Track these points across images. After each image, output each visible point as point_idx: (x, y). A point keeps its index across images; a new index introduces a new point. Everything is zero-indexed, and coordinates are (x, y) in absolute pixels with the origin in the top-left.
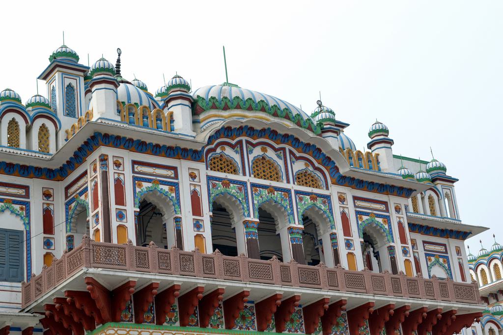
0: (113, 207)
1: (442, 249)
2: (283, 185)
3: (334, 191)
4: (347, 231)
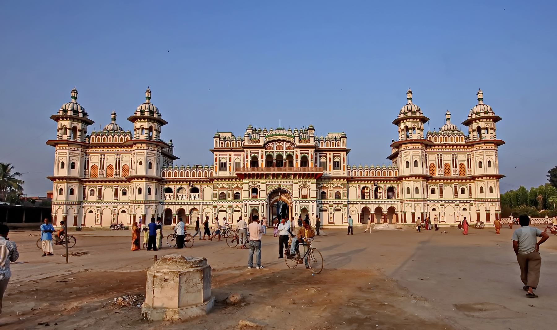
3: (295, 150)
4: (297, 158)
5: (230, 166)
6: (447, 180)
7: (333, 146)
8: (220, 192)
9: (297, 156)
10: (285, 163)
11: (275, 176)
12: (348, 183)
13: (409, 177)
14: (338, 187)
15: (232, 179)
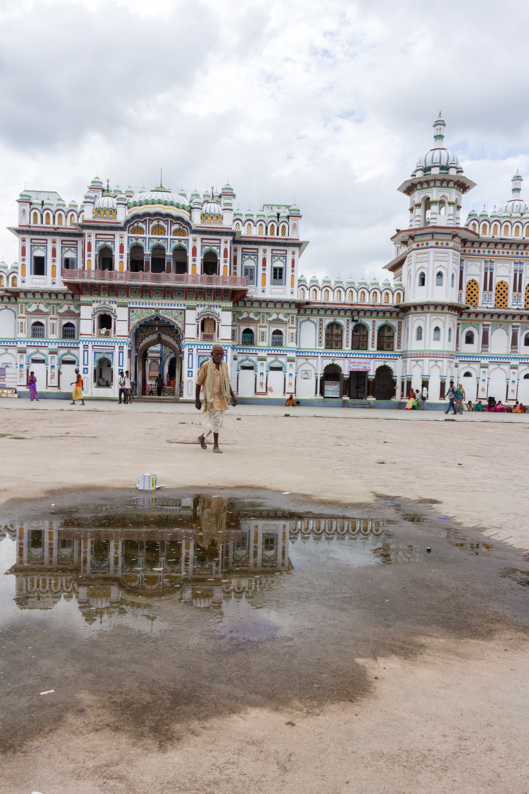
0: (87, 253)
1: (284, 252)
2: (166, 237)
3: (191, 237)
6: (499, 315)
7: (272, 234)
10: (169, 263)
11: (145, 291)
12: (299, 313)
13: (422, 306)
14: (278, 321)
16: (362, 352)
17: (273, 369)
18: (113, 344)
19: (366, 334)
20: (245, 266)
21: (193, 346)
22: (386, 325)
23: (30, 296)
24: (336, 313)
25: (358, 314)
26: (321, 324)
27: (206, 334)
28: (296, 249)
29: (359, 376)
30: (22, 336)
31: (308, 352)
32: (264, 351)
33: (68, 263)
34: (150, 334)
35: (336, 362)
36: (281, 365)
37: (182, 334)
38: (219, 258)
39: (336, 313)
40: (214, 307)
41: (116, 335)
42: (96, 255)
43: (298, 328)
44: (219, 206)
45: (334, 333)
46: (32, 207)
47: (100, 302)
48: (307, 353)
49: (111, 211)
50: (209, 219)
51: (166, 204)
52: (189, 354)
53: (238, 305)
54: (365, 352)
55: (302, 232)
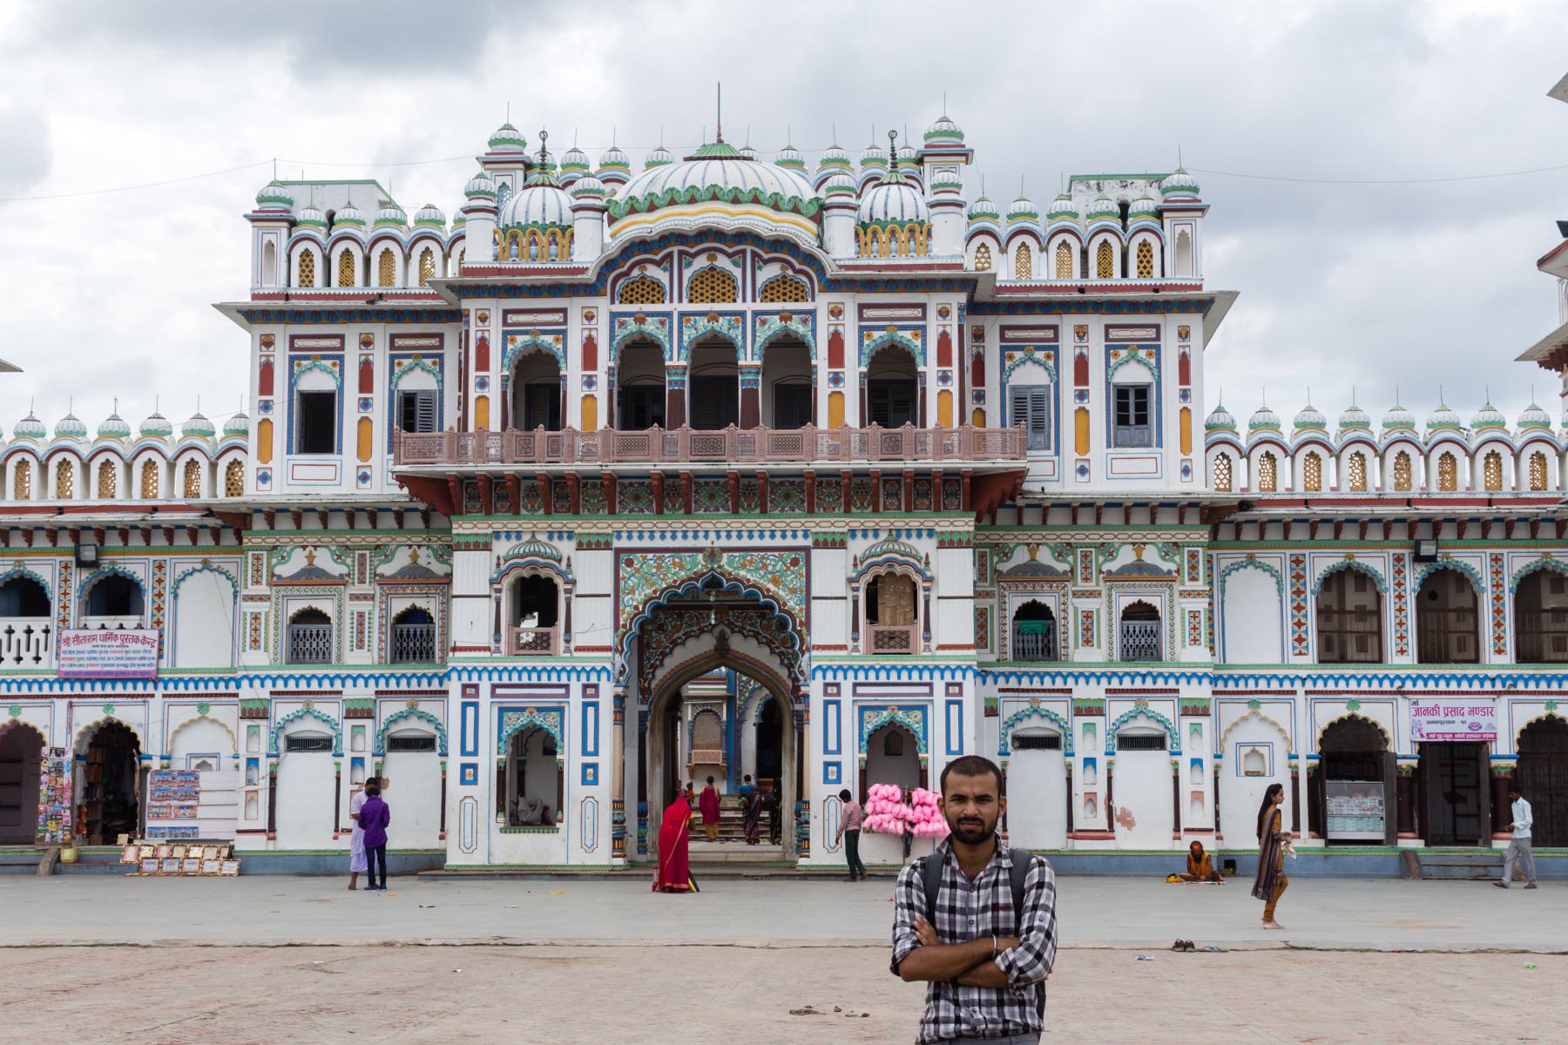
0: (473, 374)
1: (1152, 333)
2: (739, 306)
3: (822, 302)
5: (364, 417)
7: (1105, 272)
8: (295, 607)
9: (836, 343)
10: (751, 394)
11: (669, 493)
12: (1214, 541)
14: (1139, 572)
15: (373, 513)
16: (1459, 670)
17: (1130, 743)
18: (564, 677)
19: (1469, 604)
20: (1014, 388)
21: (840, 675)
22: (1544, 569)
23: (285, 524)
24: (1350, 534)
25: (1435, 535)
26: (1298, 577)
27: (886, 628)
28: (1194, 321)
29: (1453, 761)
30: (257, 659)
31: (1257, 679)
32: (1093, 681)
33: (411, 413)
34: (688, 636)
35: (1366, 711)
36: (1161, 728)
37: (799, 633)
38: (920, 369)
39: (1350, 534)
40: (909, 536)
41: (573, 645)
42: (505, 379)
43: (1215, 594)
44: (917, 193)
45: (1350, 606)
46: (297, 232)
47: (519, 535)
48: (1251, 683)
49: (554, 234)
50: (884, 237)
51: (736, 201)
52: (827, 703)
53: (993, 522)
54: (1471, 671)
55: (1213, 259)
